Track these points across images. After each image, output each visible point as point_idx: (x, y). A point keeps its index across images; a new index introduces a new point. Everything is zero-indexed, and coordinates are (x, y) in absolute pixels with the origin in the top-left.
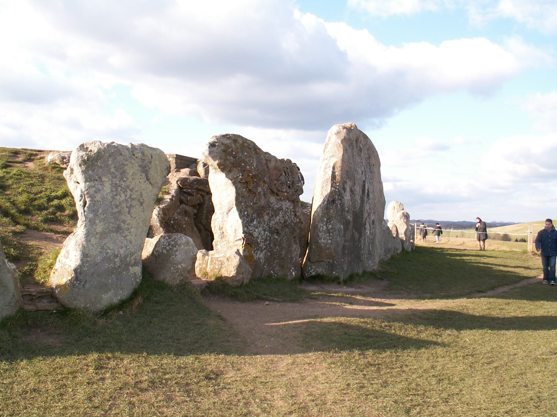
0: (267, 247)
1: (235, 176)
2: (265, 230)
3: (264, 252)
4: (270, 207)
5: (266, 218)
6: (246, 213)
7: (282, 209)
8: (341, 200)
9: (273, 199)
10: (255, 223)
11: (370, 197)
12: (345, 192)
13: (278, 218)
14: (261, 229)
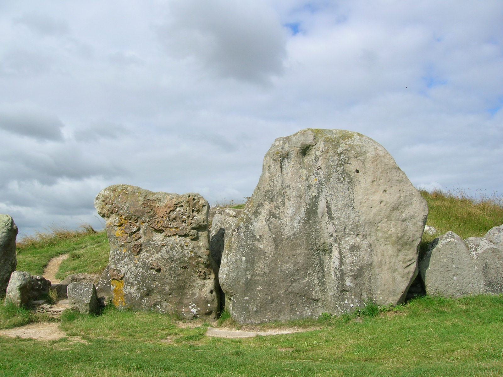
0: (139, 283)
1: (113, 221)
2: (137, 267)
3: (136, 287)
4: (151, 244)
5: (143, 255)
6: (118, 252)
7: (168, 246)
8: (247, 227)
9: (159, 238)
10: (126, 260)
11: (335, 215)
12: (256, 216)
13: (160, 253)
14: (132, 265)
